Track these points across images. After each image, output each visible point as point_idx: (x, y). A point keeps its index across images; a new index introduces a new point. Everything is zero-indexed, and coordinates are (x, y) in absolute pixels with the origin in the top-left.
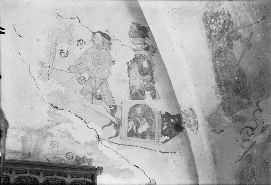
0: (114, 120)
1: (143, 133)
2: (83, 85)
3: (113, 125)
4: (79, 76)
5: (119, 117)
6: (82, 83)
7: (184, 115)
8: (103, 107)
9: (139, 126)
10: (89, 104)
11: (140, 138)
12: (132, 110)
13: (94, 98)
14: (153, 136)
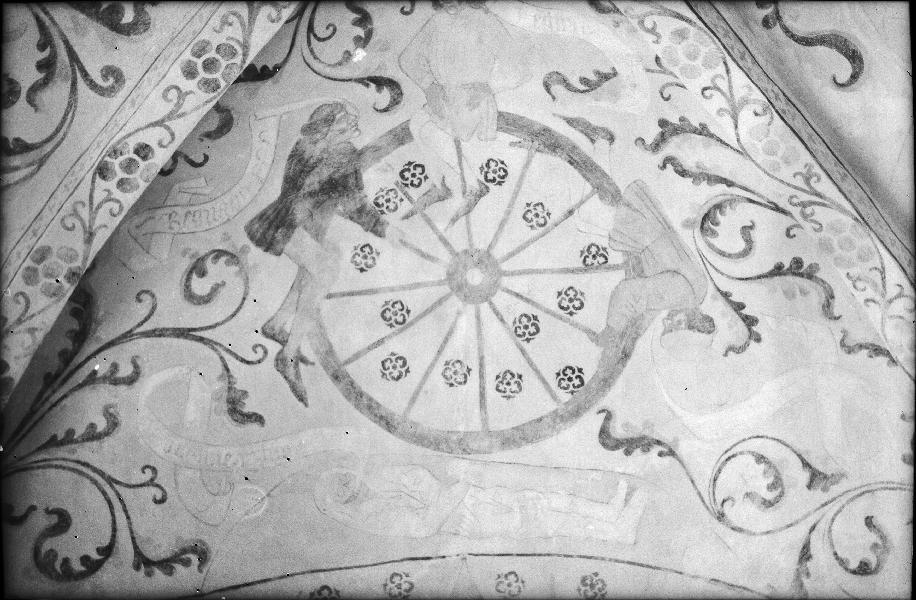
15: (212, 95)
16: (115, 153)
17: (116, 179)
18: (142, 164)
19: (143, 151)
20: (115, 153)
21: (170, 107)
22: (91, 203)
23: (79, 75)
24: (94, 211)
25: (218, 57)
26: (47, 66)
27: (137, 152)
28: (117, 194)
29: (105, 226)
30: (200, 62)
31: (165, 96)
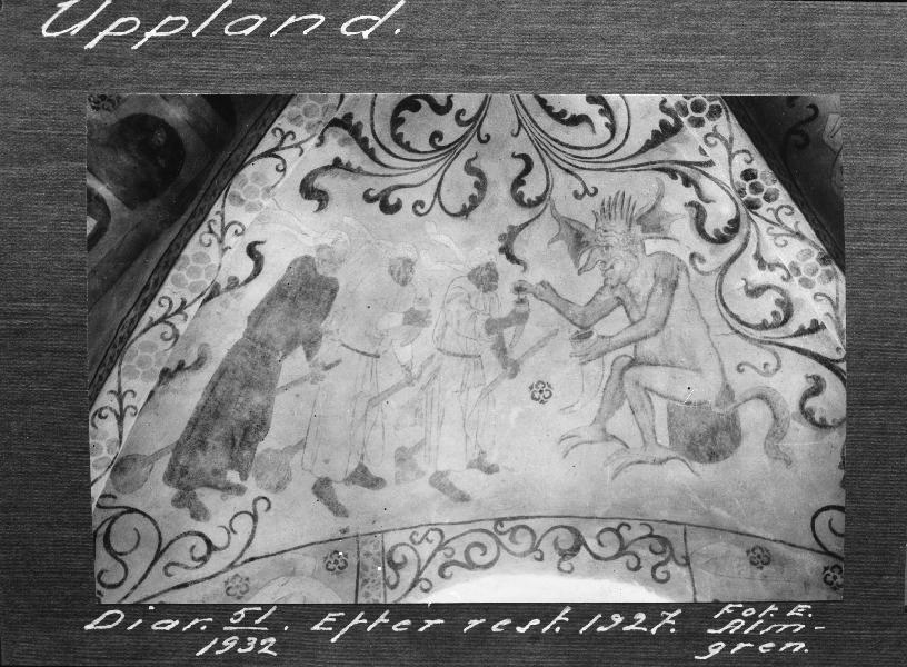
15: (724, 112)
16: (741, 192)
17: (762, 200)
18: (759, 180)
19: (748, 175)
20: (741, 192)
21: (720, 144)
22: (773, 223)
23: (703, 169)
24: (779, 223)
25: (692, 99)
26: (687, 182)
27: (747, 179)
28: (775, 205)
29: (797, 223)
30: (691, 113)
31: (711, 146)
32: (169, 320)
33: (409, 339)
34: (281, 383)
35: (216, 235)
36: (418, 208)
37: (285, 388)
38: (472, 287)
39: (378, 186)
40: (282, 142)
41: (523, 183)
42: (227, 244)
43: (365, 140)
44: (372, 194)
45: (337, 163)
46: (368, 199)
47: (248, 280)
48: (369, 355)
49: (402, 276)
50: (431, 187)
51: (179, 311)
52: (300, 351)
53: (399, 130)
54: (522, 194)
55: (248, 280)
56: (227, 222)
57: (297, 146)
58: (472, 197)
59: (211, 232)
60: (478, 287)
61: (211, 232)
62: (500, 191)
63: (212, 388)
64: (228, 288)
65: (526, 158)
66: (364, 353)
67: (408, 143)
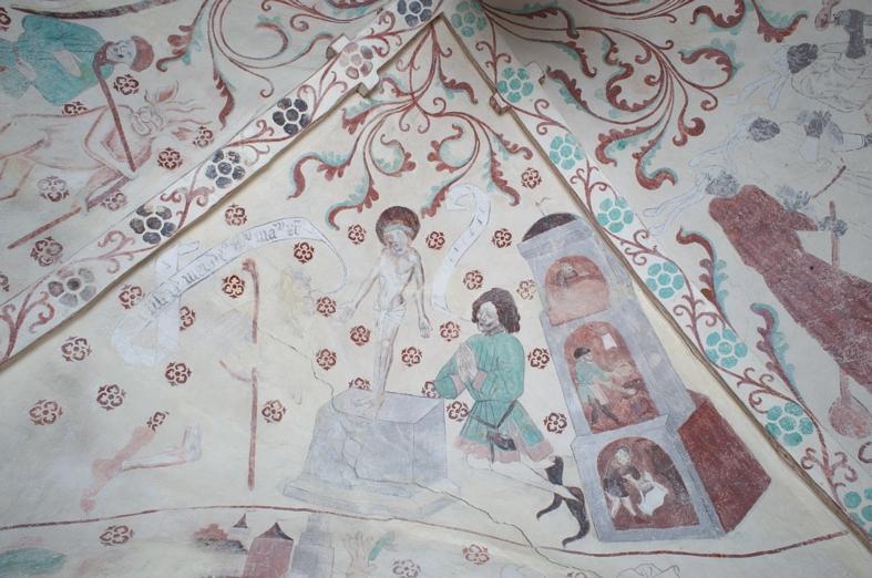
0: (569, 496)
1: (657, 511)
2: (463, 422)
3: (564, 504)
4: (449, 402)
5: (577, 483)
6: (459, 417)
7: (765, 415)
8: (527, 469)
9: (639, 495)
10: (485, 463)
11: (653, 527)
12: (604, 460)
13: (495, 447)
14: (691, 519)
32: (697, 315)
33: (838, 135)
34: (828, 260)
35: (639, 253)
36: (708, 106)
37: (835, 257)
38: (807, 71)
39: (673, 131)
40: (583, 180)
41: (720, 16)
42: (651, 247)
43: (627, 131)
44: (679, 138)
45: (636, 156)
46: (684, 141)
47: (710, 251)
48: (838, 176)
49: (769, 131)
50: (694, 94)
51: (693, 304)
52: (802, 235)
53: (630, 105)
54: (730, 18)
55: (710, 251)
56: (633, 241)
57: (590, 169)
58: (718, 62)
59: (635, 254)
60: (809, 64)
61: (635, 254)
62: (724, 36)
63: (800, 318)
64: (711, 269)
65: (698, 11)
66: (834, 180)
67: (645, 101)
